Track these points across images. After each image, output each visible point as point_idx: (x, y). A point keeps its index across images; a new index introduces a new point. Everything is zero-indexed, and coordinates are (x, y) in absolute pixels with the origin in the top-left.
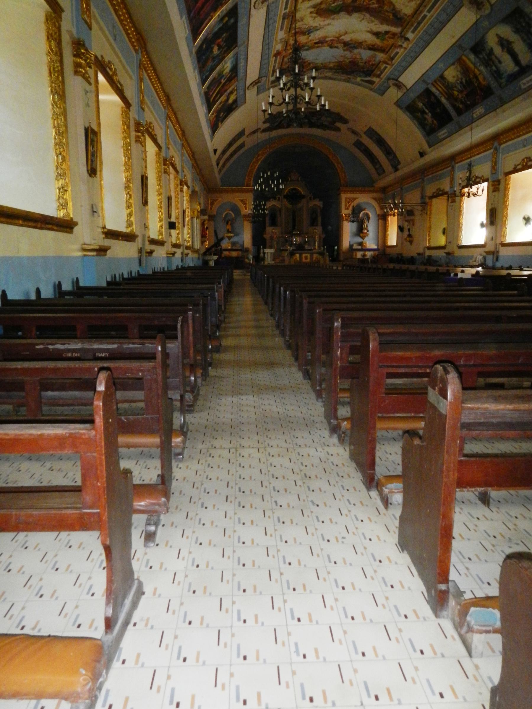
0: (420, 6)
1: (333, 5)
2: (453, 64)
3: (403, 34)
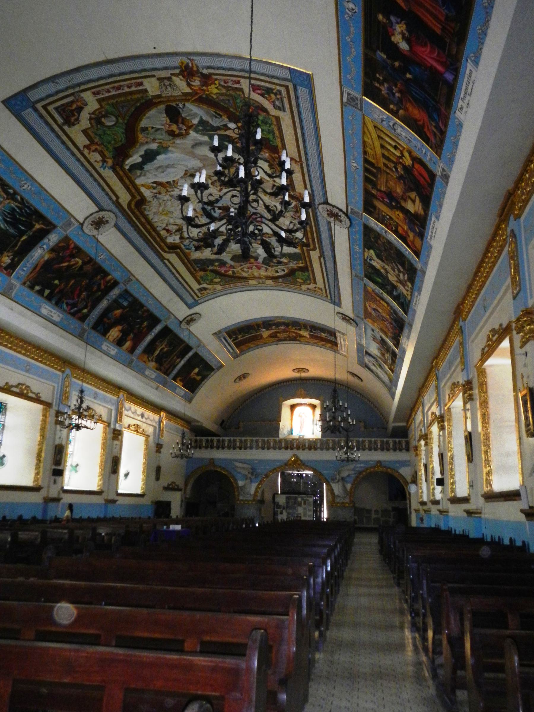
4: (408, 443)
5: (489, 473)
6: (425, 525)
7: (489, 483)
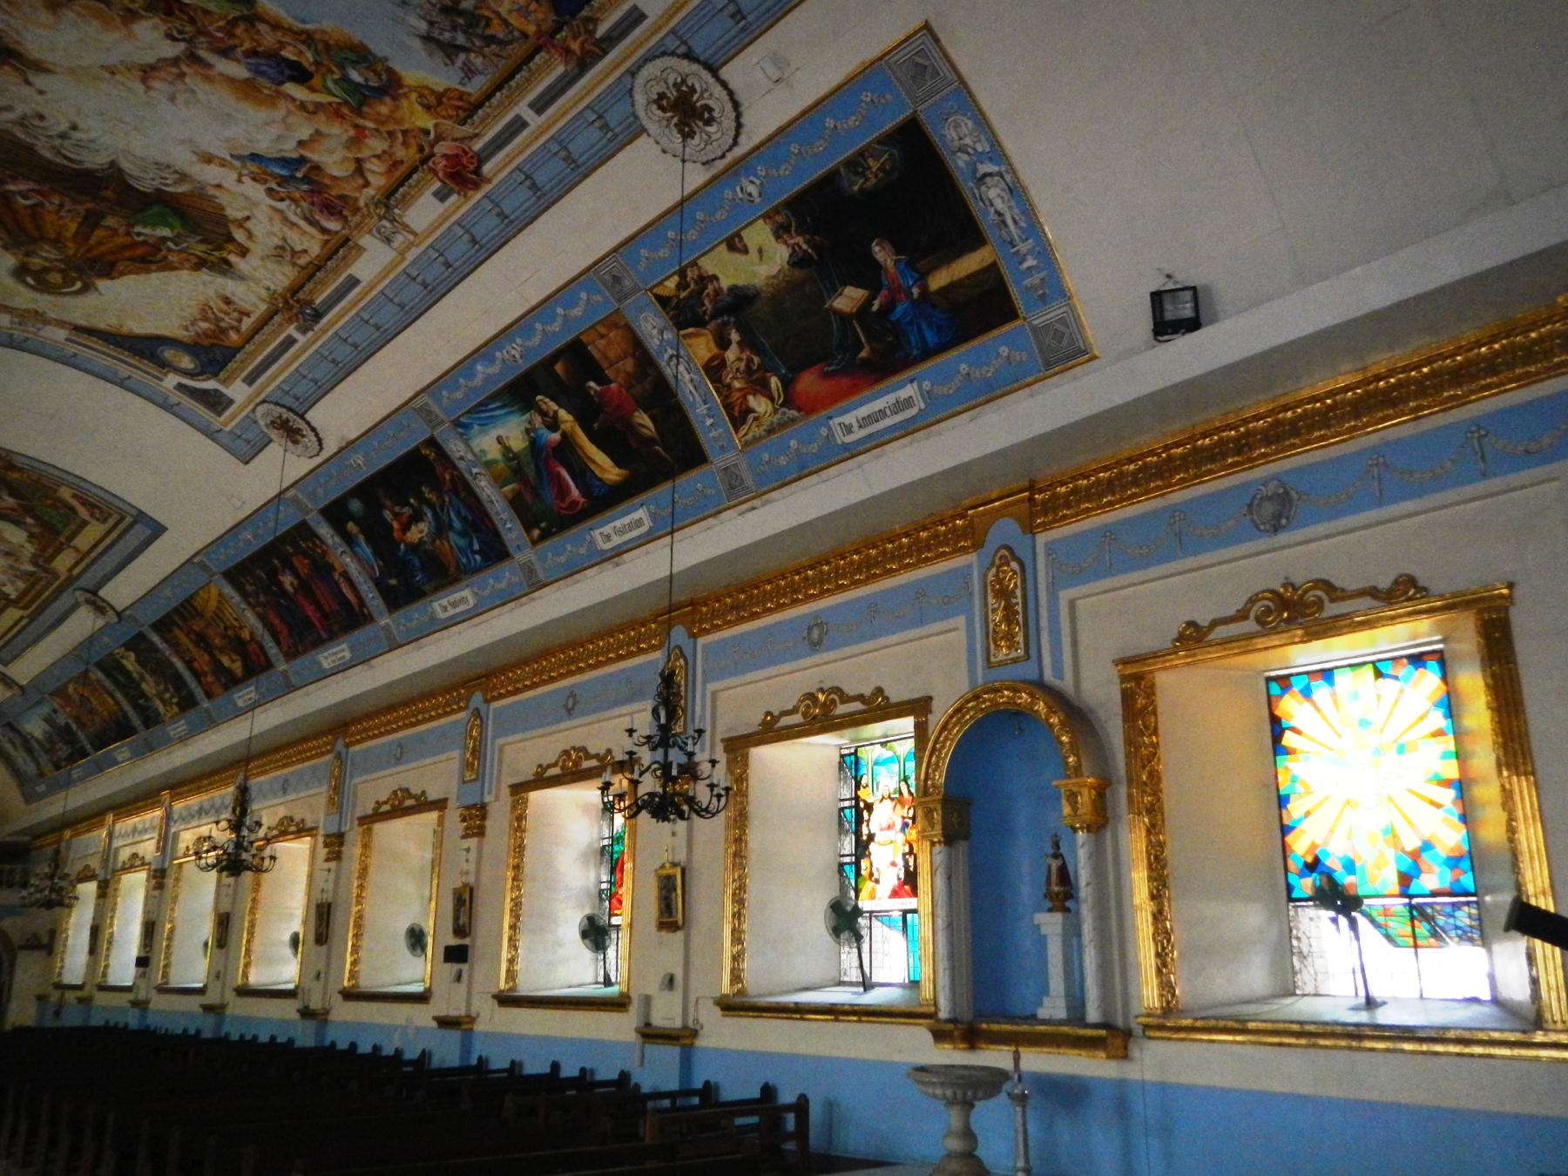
1: (165, 232)
4: (26, 874)
5: (247, 965)
6: (72, 1018)
7: (245, 975)
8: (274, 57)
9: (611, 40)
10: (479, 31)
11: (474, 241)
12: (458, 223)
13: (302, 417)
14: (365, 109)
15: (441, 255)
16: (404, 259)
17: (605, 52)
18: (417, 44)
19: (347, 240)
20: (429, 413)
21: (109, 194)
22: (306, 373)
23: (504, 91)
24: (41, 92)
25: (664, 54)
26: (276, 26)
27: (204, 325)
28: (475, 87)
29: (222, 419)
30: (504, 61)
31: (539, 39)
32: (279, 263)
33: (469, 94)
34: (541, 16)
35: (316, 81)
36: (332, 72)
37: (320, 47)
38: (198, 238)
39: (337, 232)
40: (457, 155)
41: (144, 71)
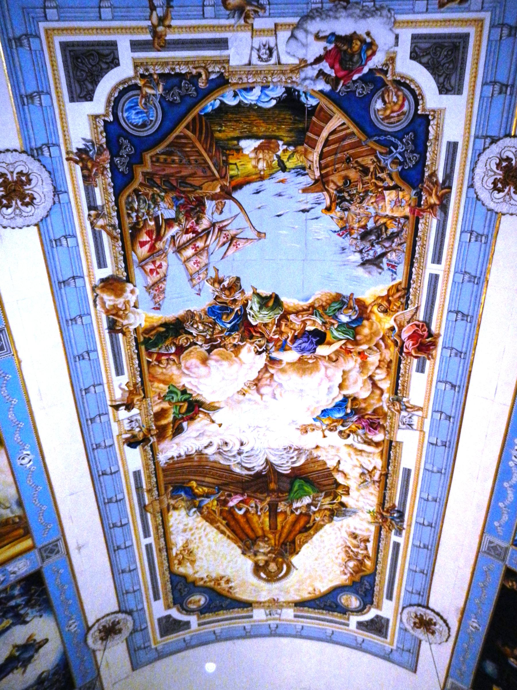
0: (166, 544)
1: (307, 500)
2: (20, 503)
3: (148, 448)
8: (304, 334)
9: (449, 176)
10: (384, 236)
11: (453, 386)
12: (439, 381)
13: (428, 607)
14: (358, 338)
15: (442, 413)
16: (424, 433)
17: (450, 188)
18: (361, 272)
19: (391, 442)
20: (495, 548)
21: (272, 486)
22: (414, 568)
23: (415, 265)
24: (220, 425)
25: (479, 155)
26: (297, 313)
27: (351, 564)
28: (400, 278)
29: (389, 640)
30: (405, 245)
31: (414, 214)
32: (367, 487)
33: (400, 283)
34: (407, 198)
35: (329, 338)
36: (333, 324)
37: (321, 311)
38: (323, 494)
39: (383, 441)
40: (414, 332)
41: (256, 385)
